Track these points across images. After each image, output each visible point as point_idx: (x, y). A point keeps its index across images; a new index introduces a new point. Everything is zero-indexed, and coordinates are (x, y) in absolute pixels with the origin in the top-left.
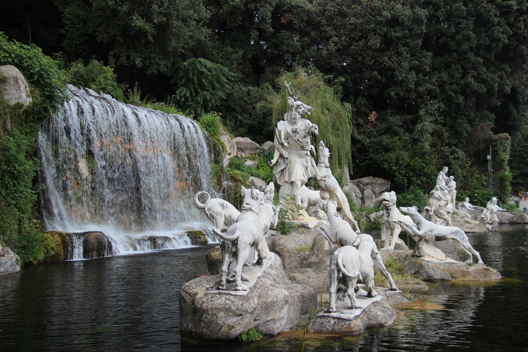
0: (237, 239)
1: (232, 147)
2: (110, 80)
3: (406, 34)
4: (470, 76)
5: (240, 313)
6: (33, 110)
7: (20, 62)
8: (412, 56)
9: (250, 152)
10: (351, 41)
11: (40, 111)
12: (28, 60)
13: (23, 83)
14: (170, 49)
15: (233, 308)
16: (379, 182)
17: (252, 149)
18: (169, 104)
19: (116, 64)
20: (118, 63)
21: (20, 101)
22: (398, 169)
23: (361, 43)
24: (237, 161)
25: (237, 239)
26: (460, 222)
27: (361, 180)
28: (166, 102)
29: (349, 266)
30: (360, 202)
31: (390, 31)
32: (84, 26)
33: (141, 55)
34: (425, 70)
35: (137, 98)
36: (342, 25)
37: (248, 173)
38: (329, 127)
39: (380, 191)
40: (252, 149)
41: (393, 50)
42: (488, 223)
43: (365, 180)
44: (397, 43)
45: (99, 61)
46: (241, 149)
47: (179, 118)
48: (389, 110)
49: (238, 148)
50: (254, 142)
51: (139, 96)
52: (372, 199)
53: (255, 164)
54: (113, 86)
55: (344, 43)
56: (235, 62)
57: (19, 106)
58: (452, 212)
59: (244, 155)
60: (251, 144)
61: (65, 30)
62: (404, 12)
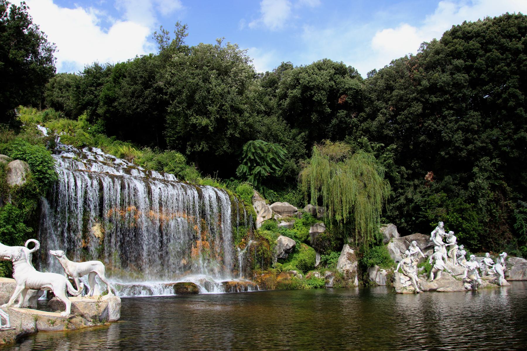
3: (448, 98)
4: (523, 130)
9: (287, 214)
10: (398, 110)
24: (271, 222)
26: (449, 279)
27: (407, 237)
28: (212, 177)
34: (474, 129)
42: (467, 282)
43: (411, 237)
50: (292, 206)
55: (392, 113)
58: (443, 269)
60: (288, 207)
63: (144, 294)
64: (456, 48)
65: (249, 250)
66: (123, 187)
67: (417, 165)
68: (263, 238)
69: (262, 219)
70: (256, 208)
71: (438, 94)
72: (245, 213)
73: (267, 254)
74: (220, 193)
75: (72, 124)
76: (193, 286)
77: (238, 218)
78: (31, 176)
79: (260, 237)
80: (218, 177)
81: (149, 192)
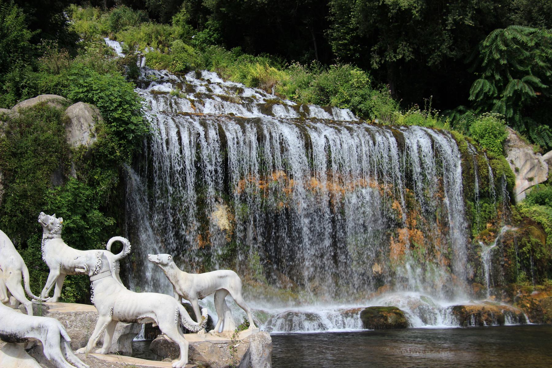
13: (86, 121)
28: (422, 109)
63: (310, 328)
65: (502, 245)
66: (260, 138)
68: (530, 220)
69: (526, 184)
70: (512, 162)
72: (491, 172)
73: (541, 251)
74: (439, 138)
75: (162, 32)
76: (396, 313)
77: (477, 185)
78: (104, 129)
79: (525, 218)
80: (433, 107)
81: (308, 145)
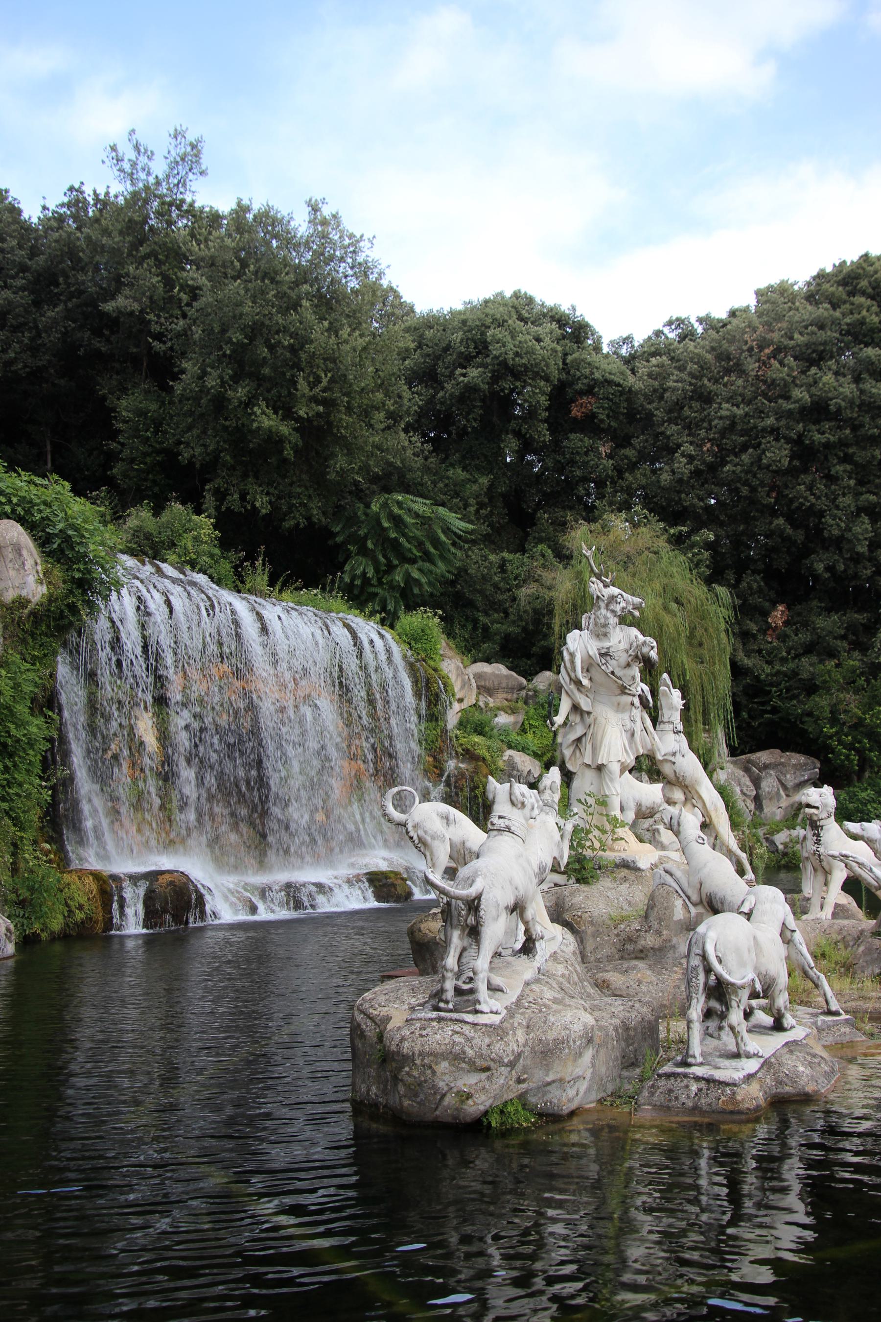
0: (479, 897)
1: (465, 684)
2: (206, 543)
3: (846, 437)
5: (485, 1064)
6: (49, 610)
7: (28, 512)
8: (861, 483)
9: (505, 695)
11: (62, 612)
12: (42, 507)
13: (32, 555)
14: (332, 476)
15: (470, 1053)
16: (794, 761)
17: (511, 690)
18: (331, 591)
19: (217, 508)
20: (223, 508)
21: (24, 593)
22: (837, 733)
23: (745, 458)
24: (477, 716)
25: (479, 897)
27: (754, 756)
28: (323, 589)
29: (731, 959)
30: (752, 806)
31: (809, 431)
32: (156, 432)
33: (272, 490)
35: (261, 580)
36: (703, 420)
37: (502, 741)
38: (683, 640)
39: (797, 781)
40: (511, 690)
41: (817, 470)
43: (764, 757)
44: (826, 458)
45: (183, 503)
46: (485, 689)
47: (353, 625)
48: (815, 603)
49: (478, 688)
51: (266, 577)
52: (778, 800)
53: (516, 723)
54: (212, 556)
55: (710, 459)
56: (472, 501)
57: (22, 603)
59: (491, 702)
60: (507, 677)
61: (119, 443)
62: (841, 390)
64: (864, 318)
67: (755, 586)
71: (827, 425)
79: (467, 751)
